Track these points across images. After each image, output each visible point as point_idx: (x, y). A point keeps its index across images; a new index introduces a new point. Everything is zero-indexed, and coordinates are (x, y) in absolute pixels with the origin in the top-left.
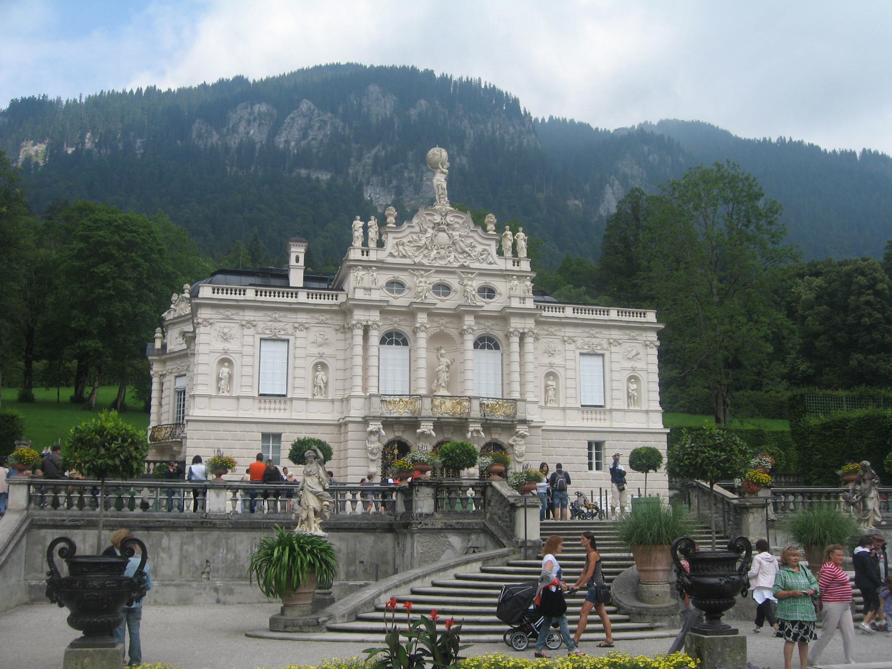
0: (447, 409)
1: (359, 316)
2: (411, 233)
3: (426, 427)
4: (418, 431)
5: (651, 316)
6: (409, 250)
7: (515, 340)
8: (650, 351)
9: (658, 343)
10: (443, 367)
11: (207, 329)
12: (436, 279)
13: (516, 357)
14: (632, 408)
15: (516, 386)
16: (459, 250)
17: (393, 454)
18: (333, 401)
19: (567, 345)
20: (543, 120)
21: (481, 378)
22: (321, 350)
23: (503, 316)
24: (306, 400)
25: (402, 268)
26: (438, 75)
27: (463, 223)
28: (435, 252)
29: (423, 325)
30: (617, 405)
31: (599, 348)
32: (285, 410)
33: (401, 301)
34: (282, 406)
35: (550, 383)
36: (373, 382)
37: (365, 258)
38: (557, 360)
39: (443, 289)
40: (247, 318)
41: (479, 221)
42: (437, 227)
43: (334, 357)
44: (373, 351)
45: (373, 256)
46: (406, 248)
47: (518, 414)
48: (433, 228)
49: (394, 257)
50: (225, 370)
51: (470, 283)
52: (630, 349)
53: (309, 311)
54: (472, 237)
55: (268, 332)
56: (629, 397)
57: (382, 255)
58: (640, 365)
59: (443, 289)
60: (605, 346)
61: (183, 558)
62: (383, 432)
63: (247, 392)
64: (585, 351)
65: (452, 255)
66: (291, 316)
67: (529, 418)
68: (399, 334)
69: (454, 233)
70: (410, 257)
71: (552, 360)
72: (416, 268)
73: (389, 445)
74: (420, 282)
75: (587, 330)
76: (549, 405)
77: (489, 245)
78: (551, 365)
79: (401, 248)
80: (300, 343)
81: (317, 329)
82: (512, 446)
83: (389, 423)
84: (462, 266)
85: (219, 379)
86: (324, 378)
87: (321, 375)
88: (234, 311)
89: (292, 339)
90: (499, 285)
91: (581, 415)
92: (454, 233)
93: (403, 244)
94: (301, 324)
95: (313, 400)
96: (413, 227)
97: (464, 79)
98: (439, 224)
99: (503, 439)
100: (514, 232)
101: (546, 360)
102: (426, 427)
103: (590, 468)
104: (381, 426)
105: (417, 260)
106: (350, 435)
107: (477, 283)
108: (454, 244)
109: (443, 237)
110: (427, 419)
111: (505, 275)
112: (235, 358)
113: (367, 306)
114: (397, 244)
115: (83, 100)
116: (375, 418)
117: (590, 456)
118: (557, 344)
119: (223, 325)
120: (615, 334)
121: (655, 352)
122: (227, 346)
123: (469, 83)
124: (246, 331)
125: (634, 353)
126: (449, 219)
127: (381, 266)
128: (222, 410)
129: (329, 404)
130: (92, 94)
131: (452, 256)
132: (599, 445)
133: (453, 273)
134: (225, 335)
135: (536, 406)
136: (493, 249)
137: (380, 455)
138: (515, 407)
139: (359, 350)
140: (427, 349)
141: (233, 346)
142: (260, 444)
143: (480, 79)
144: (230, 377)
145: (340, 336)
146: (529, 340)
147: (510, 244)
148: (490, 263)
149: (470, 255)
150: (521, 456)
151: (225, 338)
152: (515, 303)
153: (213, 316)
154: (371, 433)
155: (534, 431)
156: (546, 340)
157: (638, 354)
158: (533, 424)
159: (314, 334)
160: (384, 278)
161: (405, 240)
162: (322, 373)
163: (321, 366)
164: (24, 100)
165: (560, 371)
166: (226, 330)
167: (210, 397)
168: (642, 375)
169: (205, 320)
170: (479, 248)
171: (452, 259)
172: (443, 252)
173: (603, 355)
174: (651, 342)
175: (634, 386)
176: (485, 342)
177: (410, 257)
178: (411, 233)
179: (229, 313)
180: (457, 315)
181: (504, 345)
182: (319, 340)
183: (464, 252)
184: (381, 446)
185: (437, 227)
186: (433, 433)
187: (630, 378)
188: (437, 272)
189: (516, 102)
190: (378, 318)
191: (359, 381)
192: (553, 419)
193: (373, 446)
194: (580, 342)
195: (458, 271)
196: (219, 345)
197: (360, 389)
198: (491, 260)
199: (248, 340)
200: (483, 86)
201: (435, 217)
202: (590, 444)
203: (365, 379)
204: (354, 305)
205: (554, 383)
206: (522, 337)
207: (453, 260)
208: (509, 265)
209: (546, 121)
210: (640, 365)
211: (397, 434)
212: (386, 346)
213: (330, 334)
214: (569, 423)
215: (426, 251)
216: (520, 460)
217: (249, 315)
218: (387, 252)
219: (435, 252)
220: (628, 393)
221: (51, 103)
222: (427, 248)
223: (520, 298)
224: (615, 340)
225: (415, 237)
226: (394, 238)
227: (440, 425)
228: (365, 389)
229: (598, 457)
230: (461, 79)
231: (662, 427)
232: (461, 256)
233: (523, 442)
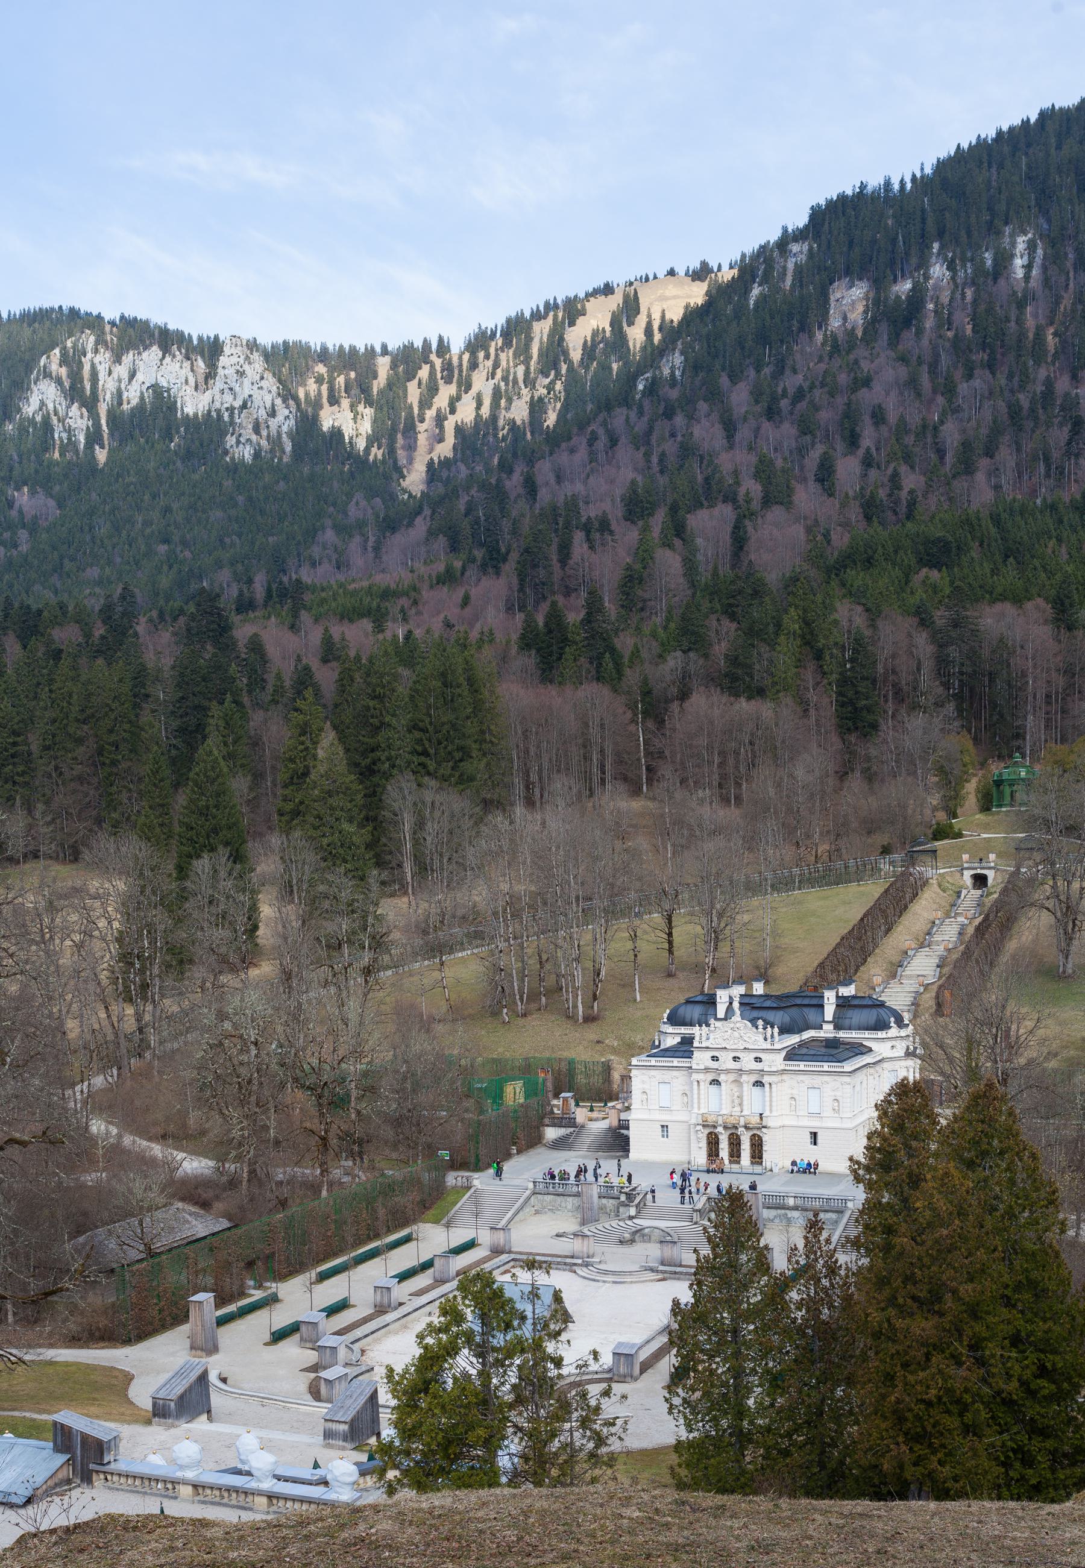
1: (695, 1076)
6: (720, 1040)
21: (753, 1103)
39: (736, 1059)
41: (753, 1022)
109: (736, 1034)
113: (698, 1071)
115: (928, 170)
130: (943, 155)
136: (761, 1038)
139: (695, 1091)
151: (643, 1082)
164: (830, 203)
176: (759, 1084)
214: (801, 1124)
217: (653, 1073)
221: (875, 196)
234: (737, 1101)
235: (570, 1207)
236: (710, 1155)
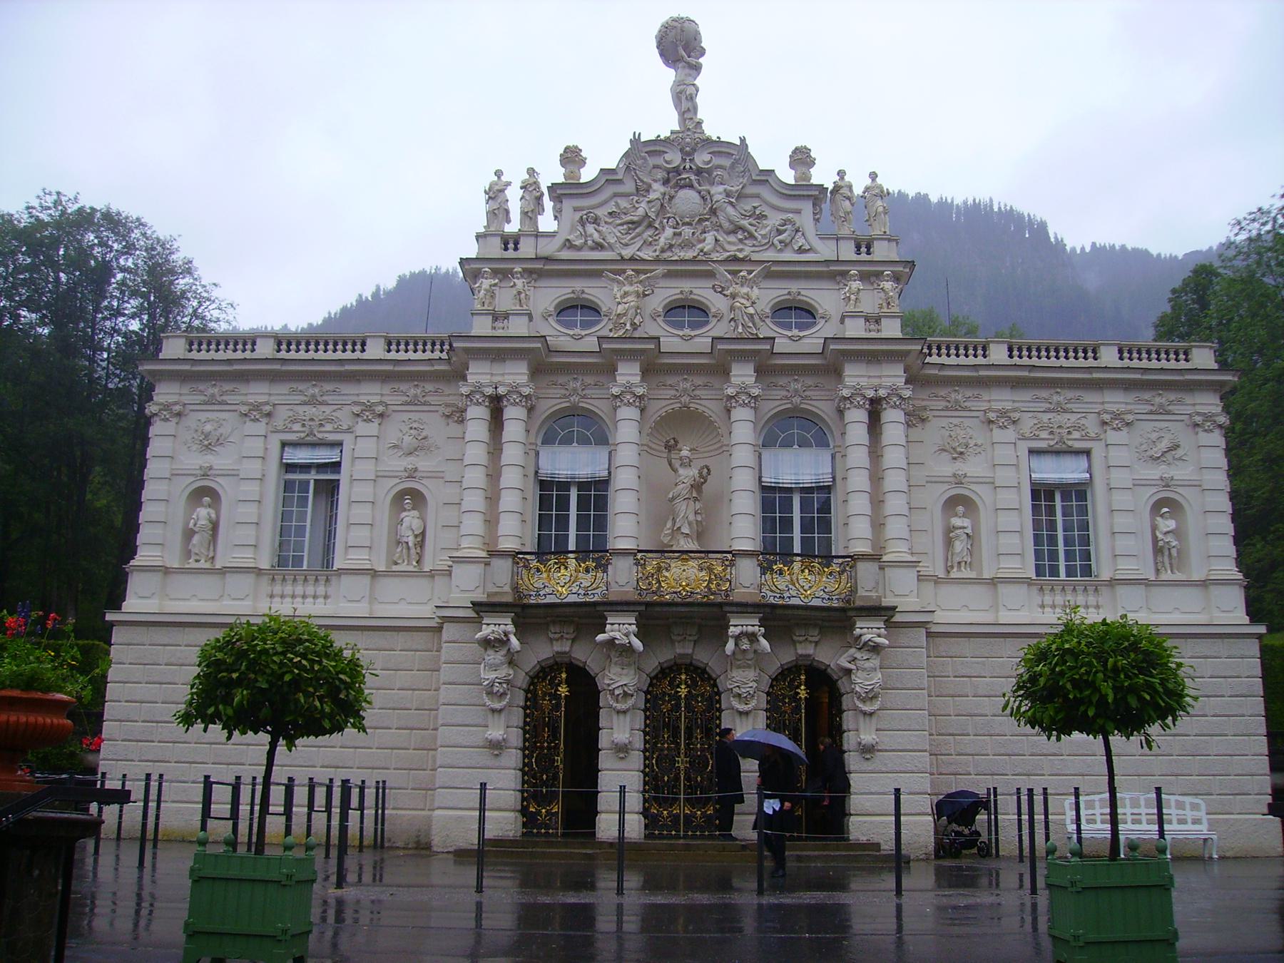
1: (480, 374)
2: (615, 195)
3: (621, 628)
4: (600, 637)
5: (1203, 357)
6: (611, 233)
7: (857, 417)
8: (1204, 438)
9: (1223, 419)
10: (683, 489)
11: (169, 428)
12: (667, 292)
14: (1167, 575)
16: (726, 225)
17: (556, 696)
19: (996, 431)
20: (1083, 249)
22: (408, 462)
24: (374, 574)
25: (592, 272)
26: (934, 199)
27: (733, 166)
28: (669, 232)
29: (628, 388)
30: (1127, 568)
31: (1076, 435)
32: (326, 597)
33: (579, 340)
34: (321, 590)
35: (957, 522)
38: (973, 467)
39: (686, 311)
40: (251, 399)
43: (436, 476)
44: (512, 454)
46: (604, 228)
47: (861, 592)
48: (666, 182)
49: (579, 249)
50: (203, 514)
51: (745, 290)
52: (1154, 436)
53: (385, 377)
54: (758, 196)
55: (297, 427)
56: (1158, 550)
58: (1180, 472)
59: (686, 311)
60: (1093, 429)
62: (513, 639)
63: (244, 558)
64: (1043, 445)
65: (710, 238)
66: (349, 389)
67: (886, 602)
68: (588, 417)
69: (714, 190)
70: (611, 247)
71: (961, 467)
73: (545, 673)
74: (626, 294)
75: (1044, 394)
76: (955, 574)
77: (798, 212)
78: (958, 480)
79: (590, 229)
80: (366, 447)
81: (406, 416)
82: (848, 672)
85: (189, 534)
86: (417, 525)
87: (411, 519)
88: (227, 387)
89: (347, 439)
90: (825, 298)
91: (1038, 599)
92: (714, 190)
93: (596, 221)
94: (369, 407)
95: (388, 574)
96: (619, 181)
97: (970, 201)
98: (677, 171)
99: (830, 656)
101: (946, 468)
102: (621, 628)
104: (511, 628)
105: (627, 253)
106: (447, 651)
107: (767, 295)
108: (713, 212)
109: (687, 200)
110: (621, 606)
111: (833, 273)
112: (224, 486)
114: (582, 222)
118: (973, 431)
119: (203, 416)
120: (1115, 401)
121: (1217, 439)
123: (976, 205)
124: (251, 428)
125: (1163, 445)
129: (424, 582)
131: (710, 238)
133: (710, 275)
134: (207, 436)
135: (911, 575)
137: (520, 698)
138: (853, 579)
139: (477, 453)
140: (644, 449)
141: (220, 460)
143: (991, 200)
144: (215, 526)
145: (454, 429)
146: (893, 418)
148: (801, 250)
149: (752, 236)
150: (871, 697)
152: (855, 329)
153: (186, 399)
154: (487, 643)
155: (906, 636)
156: (944, 422)
157: (1176, 447)
158: (898, 618)
159: (396, 430)
160: (548, 295)
161: (601, 212)
162: (415, 513)
163: (410, 498)
165: (982, 495)
166: (208, 428)
167: (166, 571)
168: (1188, 497)
169: (167, 407)
170: (774, 219)
171: (709, 244)
172: (687, 231)
173: (1087, 453)
174: (1208, 417)
175: (1171, 524)
177: (611, 247)
178: (615, 195)
179: (212, 390)
181: (837, 433)
183: (737, 228)
184: (522, 680)
186: (637, 644)
187: (1157, 506)
188: (669, 275)
189: (1043, 226)
190: (524, 379)
191: (474, 524)
192: (958, 608)
193: (493, 675)
194: (1027, 424)
195: (722, 269)
196: (194, 460)
197: (477, 542)
198: (801, 241)
199: (256, 446)
200: (996, 209)
201: (668, 157)
204: (466, 350)
205: (966, 522)
208: (847, 252)
209: (1088, 249)
210: (1180, 472)
211: (557, 647)
212: (557, 448)
213: (435, 427)
215: (650, 232)
216: (867, 708)
217: (258, 392)
218: (558, 241)
219: (669, 232)
220: (1155, 540)
222: (650, 226)
223: (867, 319)
224: (1116, 416)
225: (624, 203)
226: (576, 209)
227: (657, 617)
230: (965, 203)
231: (1246, 620)
232: (732, 238)
233: (875, 662)
234: (686, 511)
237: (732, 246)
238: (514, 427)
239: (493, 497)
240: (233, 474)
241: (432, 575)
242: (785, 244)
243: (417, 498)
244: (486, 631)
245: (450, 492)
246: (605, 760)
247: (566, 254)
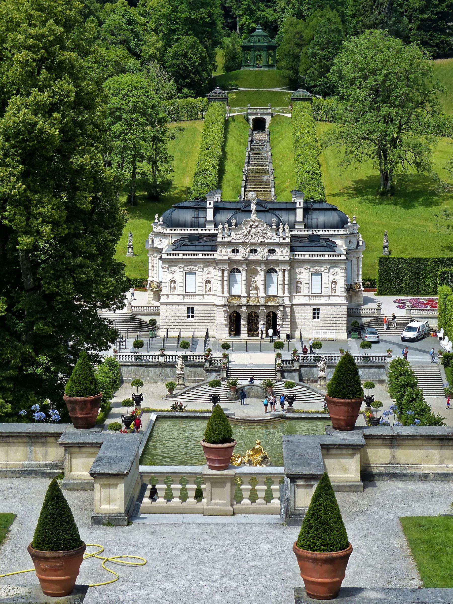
0: (252, 301)
1: (220, 266)
3: (244, 309)
6: (241, 236)
13: (281, 279)
14: (333, 294)
15: (280, 290)
18: (213, 295)
23: (277, 262)
36: (226, 290)
37: (223, 240)
39: (254, 251)
42: (251, 227)
44: (226, 279)
45: (226, 240)
50: (173, 285)
57: (230, 239)
61: (154, 373)
72: (244, 243)
83: (230, 306)
84: (261, 242)
85: (171, 288)
87: (208, 284)
89: (197, 272)
100: (284, 225)
102: (244, 309)
103: (314, 318)
109: (253, 230)
113: (222, 262)
116: (225, 305)
117: (314, 314)
121: (344, 271)
122: (172, 276)
124: (180, 270)
126: (256, 224)
127: (229, 244)
128: (173, 299)
132: (318, 309)
136: (274, 234)
139: (220, 278)
142: (186, 312)
144: (175, 287)
147: (281, 231)
166: (173, 270)
168: (339, 282)
170: (269, 234)
172: (254, 236)
180: (258, 263)
182: (207, 272)
183: (262, 236)
185: (251, 227)
196: (170, 275)
199: (181, 273)
202: (314, 309)
203: (223, 288)
206: (284, 271)
207: (258, 239)
219: (250, 237)
227: (249, 306)
228: (223, 292)
229: (318, 314)
235: (151, 374)
236: (231, 330)
237: (262, 239)
238: (226, 275)
239: (223, 284)
240: (178, 278)
241: (213, 295)
242: (271, 239)
243: (210, 282)
244: (224, 309)
245: (215, 281)
246: (242, 326)
247: (233, 241)
